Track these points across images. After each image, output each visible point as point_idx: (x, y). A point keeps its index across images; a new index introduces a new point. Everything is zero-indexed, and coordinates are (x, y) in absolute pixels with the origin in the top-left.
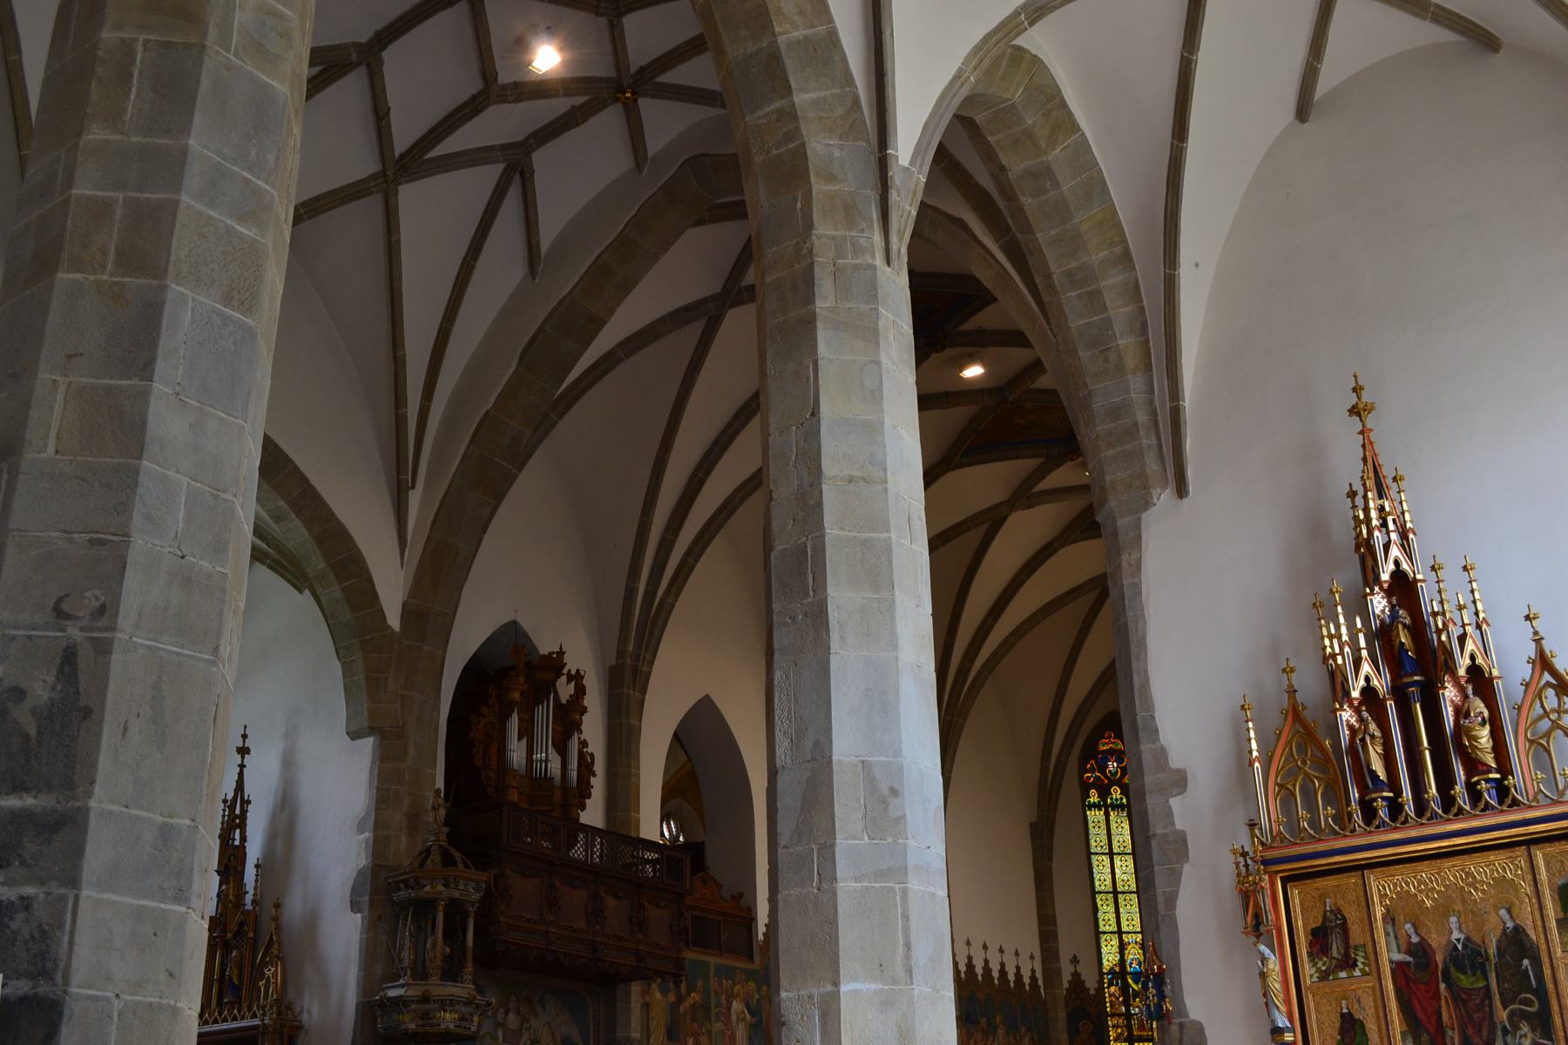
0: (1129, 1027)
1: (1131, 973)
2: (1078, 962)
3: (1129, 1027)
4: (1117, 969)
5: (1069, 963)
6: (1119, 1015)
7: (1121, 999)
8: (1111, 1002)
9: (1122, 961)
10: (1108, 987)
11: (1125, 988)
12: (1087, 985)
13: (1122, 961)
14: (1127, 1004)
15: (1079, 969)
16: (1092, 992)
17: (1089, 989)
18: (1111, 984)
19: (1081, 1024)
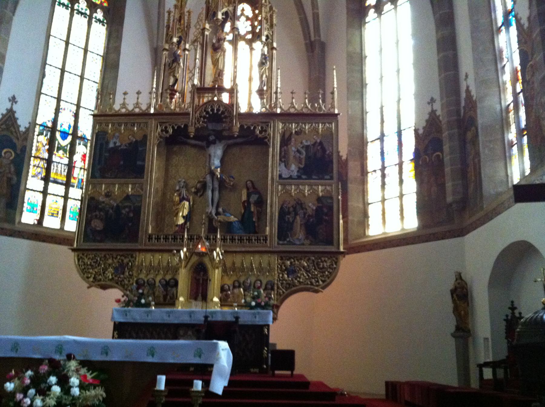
0: (48, 170)
1: (59, 131)
2: (16, 102)
3: (48, 170)
4: (50, 125)
5: (7, 100)
6: (42, 159)
7: (47, 147)
8: (37, 147)
9: (55, 122)
10: (38, 135)
11: (52, 142)
12: (19, 122)
13: (55, 122)
14: (50, 152)
15: (15, 108)
16: (22, 129)
17: (20, 126)
18: (41, 134)
19: (5, 151)
